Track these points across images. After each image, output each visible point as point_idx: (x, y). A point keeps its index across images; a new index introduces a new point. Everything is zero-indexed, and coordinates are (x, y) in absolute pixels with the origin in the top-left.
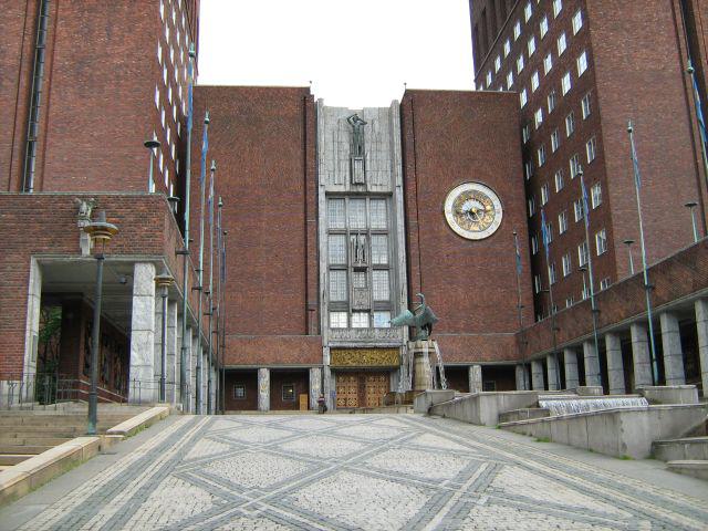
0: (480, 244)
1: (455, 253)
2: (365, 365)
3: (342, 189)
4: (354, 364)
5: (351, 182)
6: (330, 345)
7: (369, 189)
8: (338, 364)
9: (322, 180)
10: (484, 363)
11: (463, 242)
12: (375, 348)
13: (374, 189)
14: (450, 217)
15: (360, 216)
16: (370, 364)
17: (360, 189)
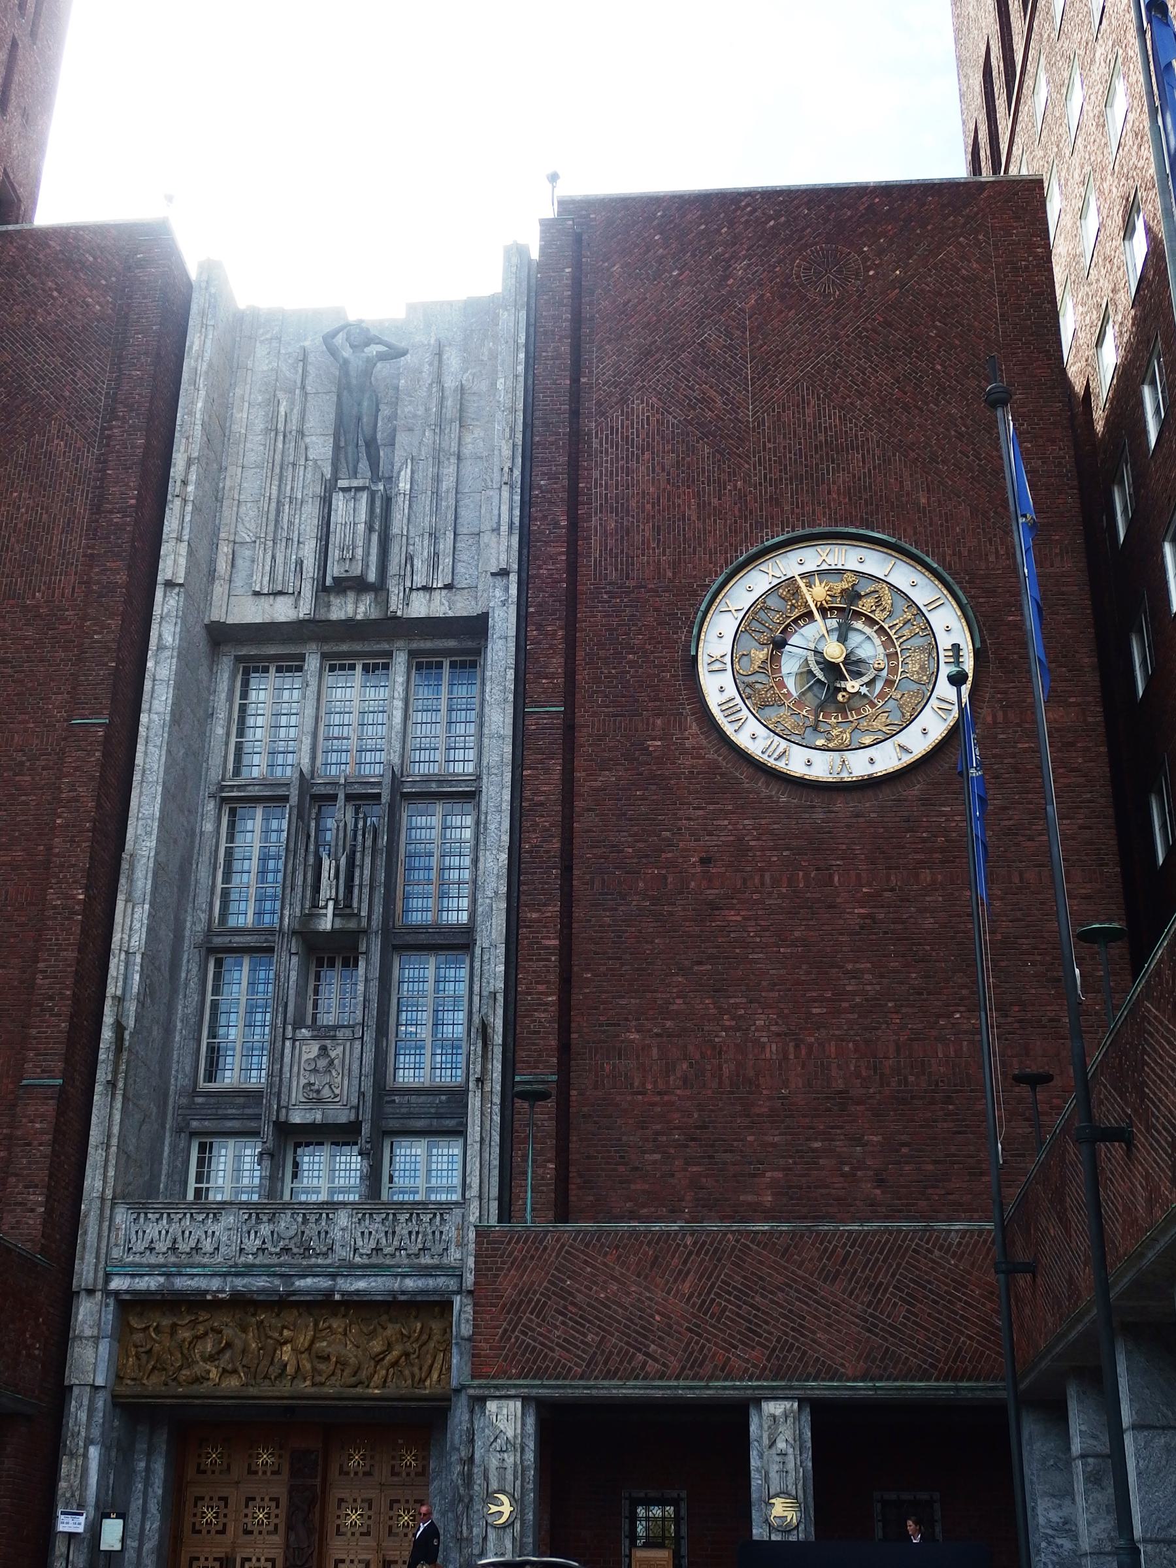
0: (868, 803)
2: (285, 1388)
3: (282, 611)
4: (233, 1383)
5: (327, 589)
6: (116, 1284)
7: (395, 604)
8: (153, 1383)
9: (173, 562)
10: (819, 1388)
12: (323, 1305)
13: (419, 607)
14: (717, 688)
15: (360, 720)
16: (305, 1386)
17: (359, 608)
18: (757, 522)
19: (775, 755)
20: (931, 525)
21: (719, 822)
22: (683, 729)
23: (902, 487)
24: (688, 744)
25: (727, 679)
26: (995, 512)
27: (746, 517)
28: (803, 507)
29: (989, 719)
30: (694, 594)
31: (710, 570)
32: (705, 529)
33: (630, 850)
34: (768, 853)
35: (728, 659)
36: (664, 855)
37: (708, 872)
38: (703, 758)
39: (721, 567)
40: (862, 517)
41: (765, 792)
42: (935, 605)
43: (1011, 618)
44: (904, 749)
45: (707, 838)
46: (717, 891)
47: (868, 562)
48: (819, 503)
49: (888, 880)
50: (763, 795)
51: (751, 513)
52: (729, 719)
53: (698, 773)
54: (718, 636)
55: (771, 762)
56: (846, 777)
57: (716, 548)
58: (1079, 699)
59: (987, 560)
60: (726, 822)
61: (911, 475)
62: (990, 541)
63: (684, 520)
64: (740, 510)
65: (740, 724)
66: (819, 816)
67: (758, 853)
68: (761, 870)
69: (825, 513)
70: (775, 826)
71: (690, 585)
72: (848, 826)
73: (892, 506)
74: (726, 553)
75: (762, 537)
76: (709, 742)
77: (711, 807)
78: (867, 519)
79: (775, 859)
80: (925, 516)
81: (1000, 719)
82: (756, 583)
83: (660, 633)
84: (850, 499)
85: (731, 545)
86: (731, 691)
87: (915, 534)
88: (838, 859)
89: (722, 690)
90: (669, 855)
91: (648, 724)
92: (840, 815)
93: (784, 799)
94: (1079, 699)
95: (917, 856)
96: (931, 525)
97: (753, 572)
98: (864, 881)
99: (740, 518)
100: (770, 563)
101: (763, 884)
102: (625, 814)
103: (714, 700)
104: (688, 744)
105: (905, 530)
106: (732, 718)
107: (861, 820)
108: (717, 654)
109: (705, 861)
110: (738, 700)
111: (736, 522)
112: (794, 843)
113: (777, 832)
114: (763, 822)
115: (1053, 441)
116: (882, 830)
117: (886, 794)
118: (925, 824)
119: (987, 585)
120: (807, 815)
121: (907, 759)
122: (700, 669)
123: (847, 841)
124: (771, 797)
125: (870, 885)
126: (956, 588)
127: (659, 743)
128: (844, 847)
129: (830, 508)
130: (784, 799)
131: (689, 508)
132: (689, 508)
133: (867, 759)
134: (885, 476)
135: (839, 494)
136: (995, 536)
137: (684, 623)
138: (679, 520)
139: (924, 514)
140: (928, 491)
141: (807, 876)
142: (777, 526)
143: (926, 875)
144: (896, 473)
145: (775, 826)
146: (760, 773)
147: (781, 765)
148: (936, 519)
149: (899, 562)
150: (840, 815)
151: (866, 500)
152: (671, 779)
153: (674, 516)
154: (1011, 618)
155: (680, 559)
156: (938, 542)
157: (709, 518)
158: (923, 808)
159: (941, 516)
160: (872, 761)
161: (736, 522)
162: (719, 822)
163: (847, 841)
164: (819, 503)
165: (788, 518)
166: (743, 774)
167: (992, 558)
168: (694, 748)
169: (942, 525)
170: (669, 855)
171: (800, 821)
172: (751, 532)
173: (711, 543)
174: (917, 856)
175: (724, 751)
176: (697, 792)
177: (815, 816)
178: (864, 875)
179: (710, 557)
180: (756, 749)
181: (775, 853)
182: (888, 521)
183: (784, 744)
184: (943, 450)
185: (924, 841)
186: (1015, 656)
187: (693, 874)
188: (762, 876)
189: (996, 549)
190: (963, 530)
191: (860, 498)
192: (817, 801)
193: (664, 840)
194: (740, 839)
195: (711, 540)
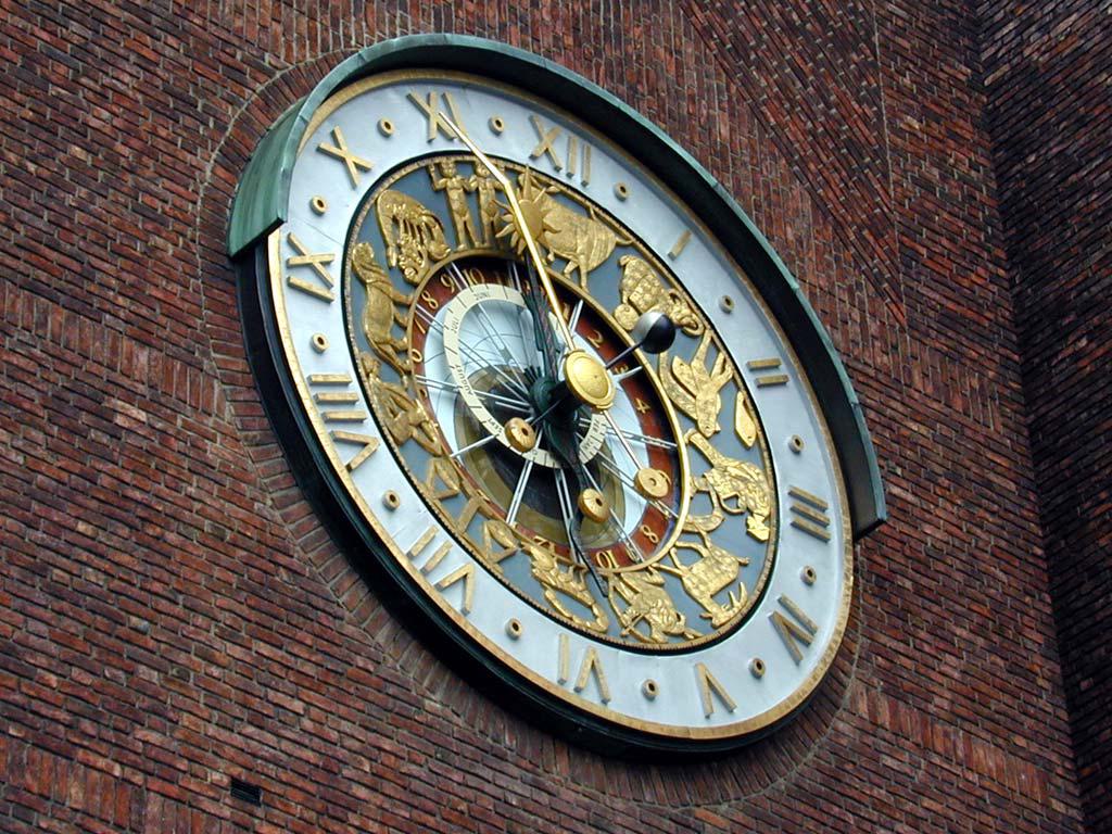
11: (438, 700)
14: (313, 339)
23: (679, 75)
24: (215, 450)
25: (330, 323)
29: (863, 707)
30: (235, 73)
31: (276, 39)
33: (53, 679)
35: (334, 274)
36: (141, 733)
45: (250, 730)
54: (316, 209)
56: (589, 701)
58: (1034, 748)
60: (298, 706)
61: (698, 60)
70: (414, 769)
74: (312, 18)
77: (265, 650)
81: (885, 717)
83: (154, 133)
84: (578, 43)
89: (318, 347)
90: (154, 737)
91: (114, 351)
94: (1034, 748)
100: (435, 92)
102: (40, 570)
103: (302, 366)
108: (313, 254)
115: (955, 137)
117: (657, 795)
120: (487, 774)
127: (143, 416)
134: (648, 28)
135: (555, 18)
139: (724, 160)
140: (732, 115)
144: (668, 40)
145: (414, 769)
151: (609, 64)
152: (166, 527)
159: (756, 184)
162: (280, 698)
166: (347, 591)
170: (154, 737)
184: (760, 41)
189: (863, 318)
191: (598, 53)
193: (143, 689)
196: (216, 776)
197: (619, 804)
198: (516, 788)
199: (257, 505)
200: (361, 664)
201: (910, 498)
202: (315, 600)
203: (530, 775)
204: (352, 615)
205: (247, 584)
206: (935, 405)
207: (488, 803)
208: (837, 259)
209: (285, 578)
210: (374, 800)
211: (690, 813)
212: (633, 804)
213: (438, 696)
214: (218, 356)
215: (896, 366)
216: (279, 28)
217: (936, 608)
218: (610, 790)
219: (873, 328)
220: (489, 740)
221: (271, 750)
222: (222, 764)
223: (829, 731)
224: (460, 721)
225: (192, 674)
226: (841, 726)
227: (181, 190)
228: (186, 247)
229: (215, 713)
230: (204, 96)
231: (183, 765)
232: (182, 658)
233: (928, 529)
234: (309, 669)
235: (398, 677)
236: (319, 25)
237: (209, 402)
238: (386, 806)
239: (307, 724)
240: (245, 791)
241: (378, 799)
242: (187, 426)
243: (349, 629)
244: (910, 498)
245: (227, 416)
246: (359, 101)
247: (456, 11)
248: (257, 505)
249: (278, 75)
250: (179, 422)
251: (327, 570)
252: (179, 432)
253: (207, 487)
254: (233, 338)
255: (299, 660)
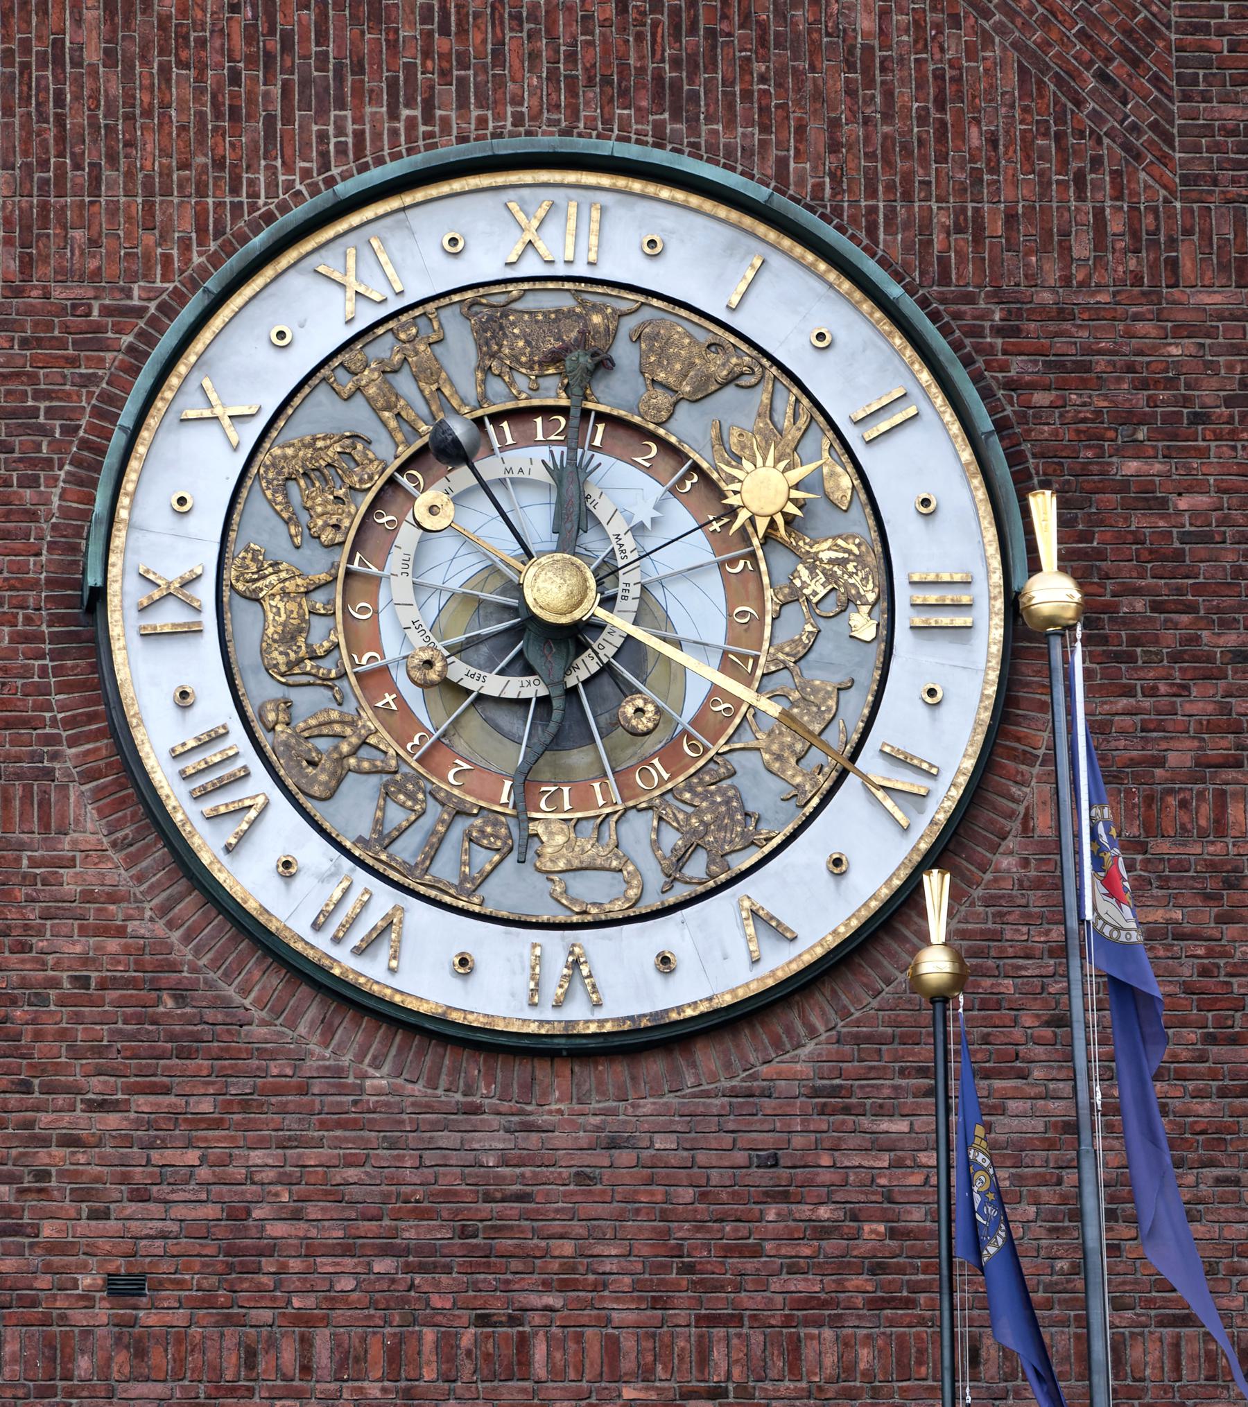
0: (648, 1101)
1: (240, 1253)
18: (305, 82)
19: (356, 938)
20: (887, 117)
21: (170, 1156)
22: (51, 822)
25: (201, 664)
26: (1102, 77)
27: (269, 57)
28: (462, 31)
30: (93, 340)
31: (148, 257)
32: (129, 99)
34: (326, 1264)
35: (205, 592)
37: (134, 1322)
38: (121, 932)
39: (185, 246)
40: (658, 77)
41: (319, 1054)
42: (889, 420)
43: (1132, 466)
44: (769, 925)
45: (132, 1208)
46: (159, 1389)
47: (676, 253)
48: (516, 18)
49: (704, 1358)
50: (310, 1066)
51: (287, 45)
52: (208, 806)
53: (103, 985)
55: (343, 960)
56: (579, 1015)
57: (166, 173)
59: (1065, 250)
60: (192, 1156)
62: (1080, 179)
63: (59, 62)
64: (251, 34)
65: (245, 826)
66: (491, 1141)
67: (295, 1264)
68: (304, 1320)
69: (534, 56)
71: (79, 307)
72: (582, 1178)
73: (763, 41)
74: (201, 192)
75: (323, 137)
76: (140, 879)
77: (142, 1102)
78: (676, 85)
79: (347, 1283)
80: (869, 83)
82: (305, 312)
85: (219, 164)
86: (216, 706)
87: (834, 147)
88: (547, 1286)
92: (558, 1138)
93: (378, 1080)
95: (798, 1284)
96: (887, 117)
97: (295, 281)
98: (627, 1364)
99: (251, 60)
101: (306, 1370)
103: (158, 738)
104: (70, 882)
105: (801, 129)
106: (220, 801)
107: (625, 1157)
108: (170, 571)
109: (125, 1287)
110: (238, 738)
111: (235, 78)
112: (411, 1232)
113: (355, 1192)
114: (311, 1156)
116: (687, 1194)
118: (826, 1176)
119: (1060, 344)
121: (782, 962)
122: (115, 631)
123: (578, 1228)
124: (339, 1072)
125: (646, 1374)
126: (960, 375)
128: (567, 1247)
129: (552, 38)
130: (378, 1080)
131: (78, 22)
132: (78, 22)
133: (652, 960)
136: (1096, 162)
137: (56, 446)
138: (42, 65)
139: (867, 71)
141: (447, 1347)
142: (375, 97)
143: (822, 1348)
145: (352, 1173)
146: (304, 989)
147: (372, 972)
148: (905, 95)
149: (776, 260)
150: (558, 1138)
152: (14, 1002)
153: (25, 46)
154: (1132, 466)
155: (44, 207)
156: (907, 178)
157: (145, 60)
158: (821, 1123)
159: (921, 85)
160: (665, 962)
161: (235, 78)
162: (170, 1156)
163: (578, 1228)
164: (516, 18)
165: (410, 68)
166: (250, 991)
167: (1082, 248)
168: (88, 896)
169: (923, 119)
171: (430, 1158)
172: (288, 120)
173: (150, 156)
174: (798, 1284)
175: (189, 907)
176: (99, 1052)
177: (479, 1141)
178: (628, 1343)
179: (149, 207)
180: (291, 912)
181: (349, 1263)
182: (747, 95)
183: (385, 899)
185: (822, 1232)
186: (1140, 604)
187: (87, 1333)
188: (306, 1343)
190: (993, 141)
192: (485, 1094)
194: (238, 1214)
195: (151, 143)
196: (85, 1281)
197: (648, 1105)
198: (491, 1141)
199: (131, 925)
200: (275, 1072)
201: (1158, 467)
202: (209, 1015)
203: (515, 1119)
204: (264, 1014)
205: (120, 1031)
206: (1218, 298)
207: (450, 1179)
208: (1059, 137)
209: (170, 1003)
210: (293, 1233)
211: (753, 1077)
212: (670, 1099)
213: (386, 1069)
214: (73, 750)
215: (1154, 266)
216: (150, 238)
217: (1185, 618)
218: (631, 1095)
219: (1116, 225)
220: (458, 1097)
221: (159, 1224)
222: (92, 1261)
223: (988, 876)
224: (418, 1088)
225: (53, 1170)
226: (1006, 862)
227: (18, 544)
228: (28, 620)
229: (84, 1205)
230: (48, 395)
231: (44, 1281)
232: (43, 1157)
233: (1183, 503)
234: (206, 1106)
235: (327, 1068)
236: (210, 200)
237: (63, 816)
238: (313, 1233)
239: (204, 1173)
240: (125, 1287)
241: (301, 1228)
242: (34, 863)
243: (261, 1032)
244: (1158, 467)
245: (89, 825)
246: (250, 307)
247: (423, 65)
248: (131, 925)
249: (152, 306)
250: (25, 862)
251: (225, 974)
252: (25, 876)
253: (65, 930)
254: (91, 717)
255: (192, 1100)
